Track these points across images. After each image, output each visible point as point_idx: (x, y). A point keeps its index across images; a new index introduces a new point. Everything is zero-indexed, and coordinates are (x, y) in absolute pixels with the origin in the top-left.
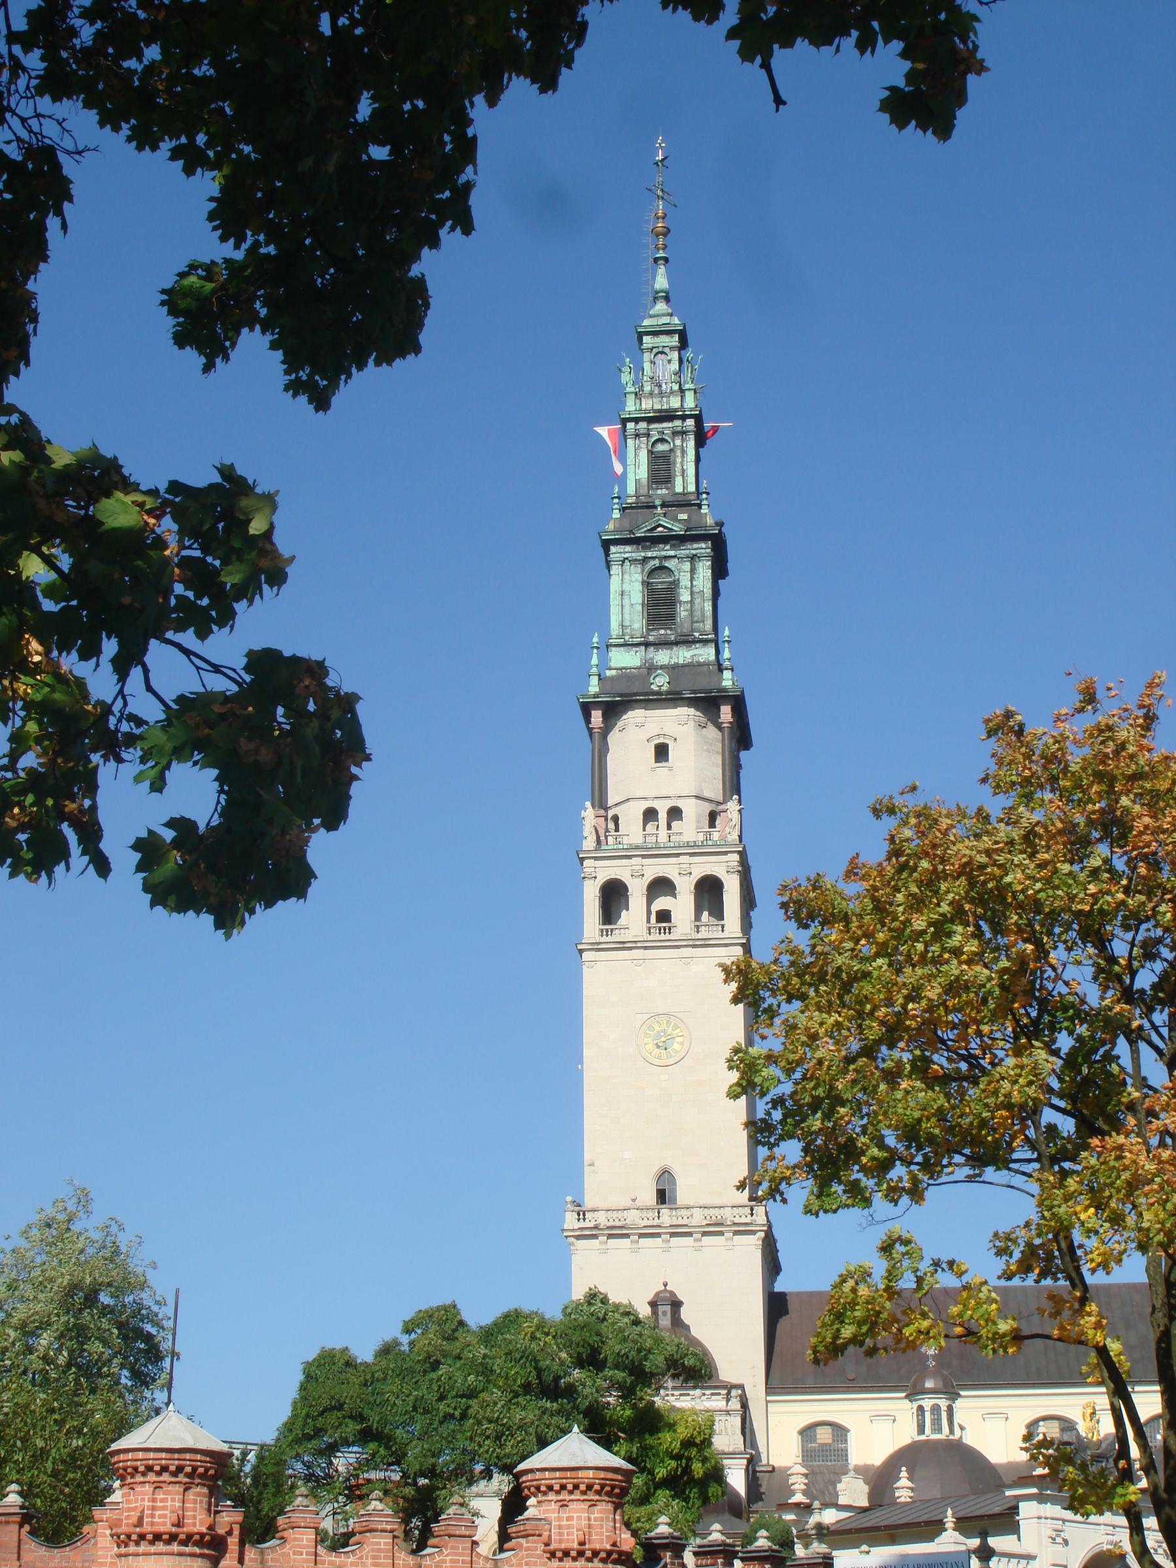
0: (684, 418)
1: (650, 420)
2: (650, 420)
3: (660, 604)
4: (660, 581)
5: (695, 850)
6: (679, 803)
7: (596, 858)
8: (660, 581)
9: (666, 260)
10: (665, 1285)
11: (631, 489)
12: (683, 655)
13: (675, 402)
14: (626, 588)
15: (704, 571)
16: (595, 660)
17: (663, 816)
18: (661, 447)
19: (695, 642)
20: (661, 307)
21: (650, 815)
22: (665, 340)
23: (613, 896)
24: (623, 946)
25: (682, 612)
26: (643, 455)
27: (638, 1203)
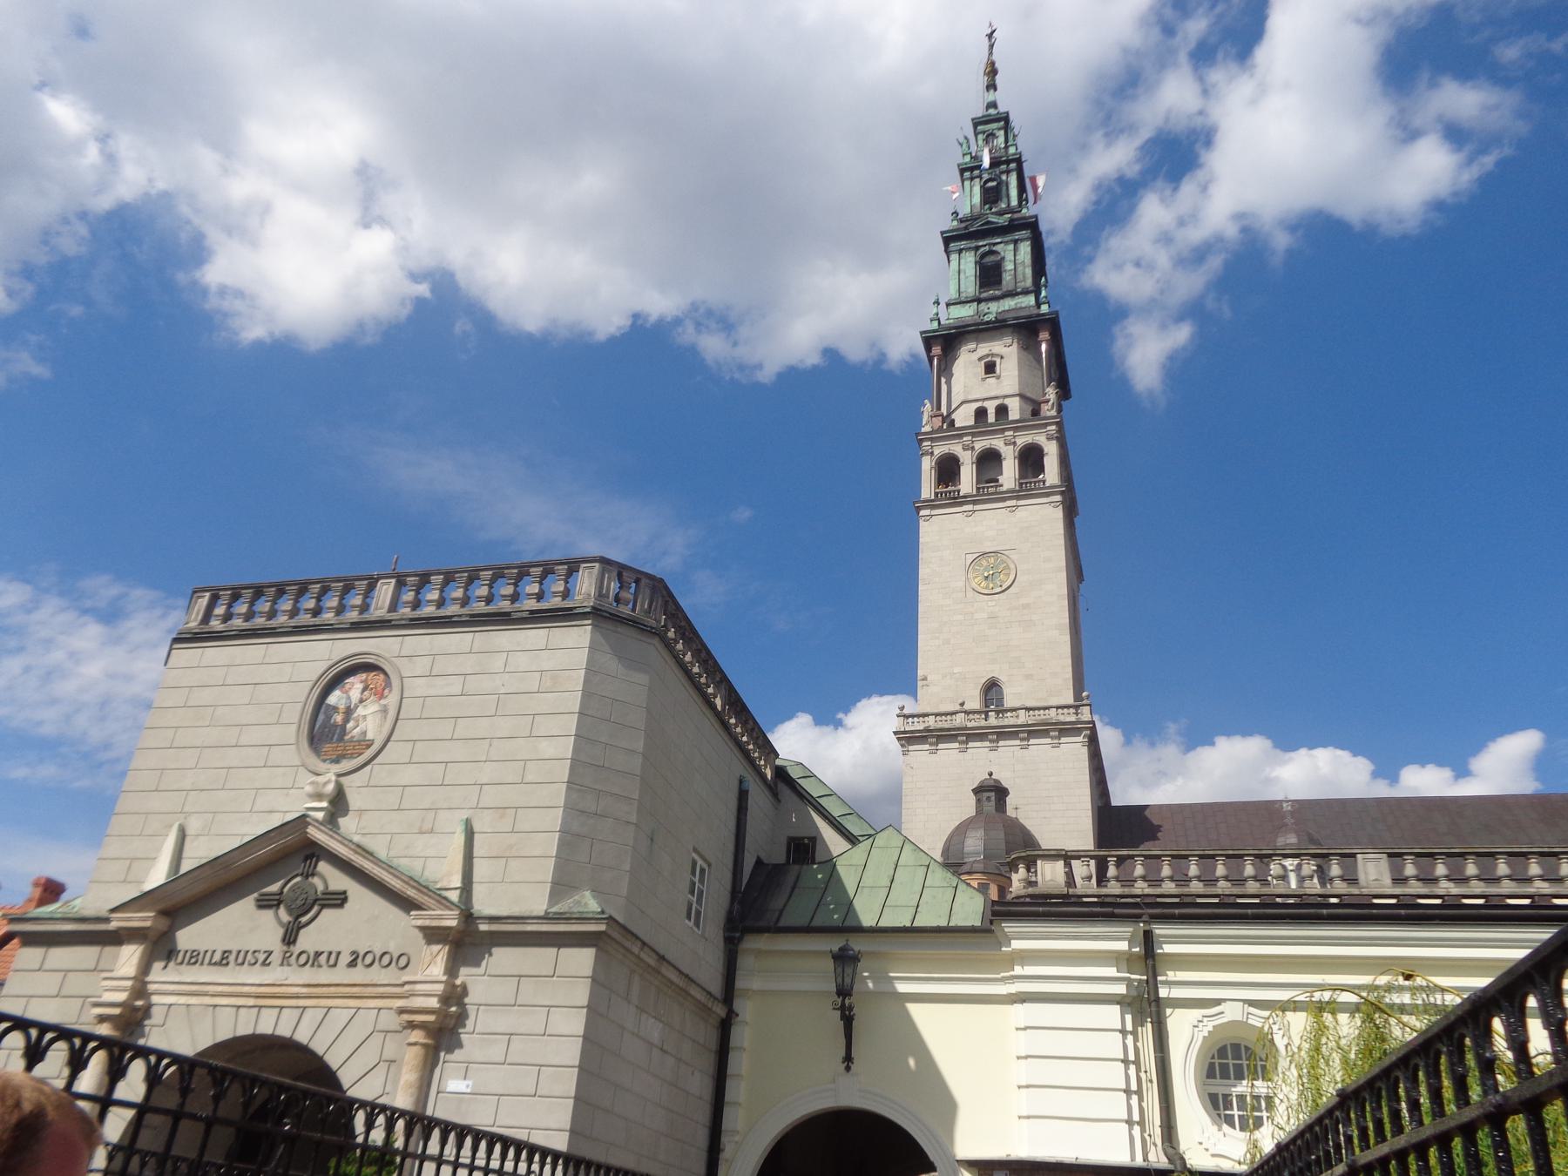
0: (1008, 162)
3: (990, 275)
4: (990, 259)
5: (1019, 427)
6: (1007, 401)
8: (990, 259)
10: (991, 774)
12: (1008, 304)
15: (1025, 249)
19: (1017, 294)
21: (981, 414)
22: (995, 125)
23: (948, 470)
24: (957, 500)
25: (1007, 278)
26: (977, 190)
27: (966, 707)
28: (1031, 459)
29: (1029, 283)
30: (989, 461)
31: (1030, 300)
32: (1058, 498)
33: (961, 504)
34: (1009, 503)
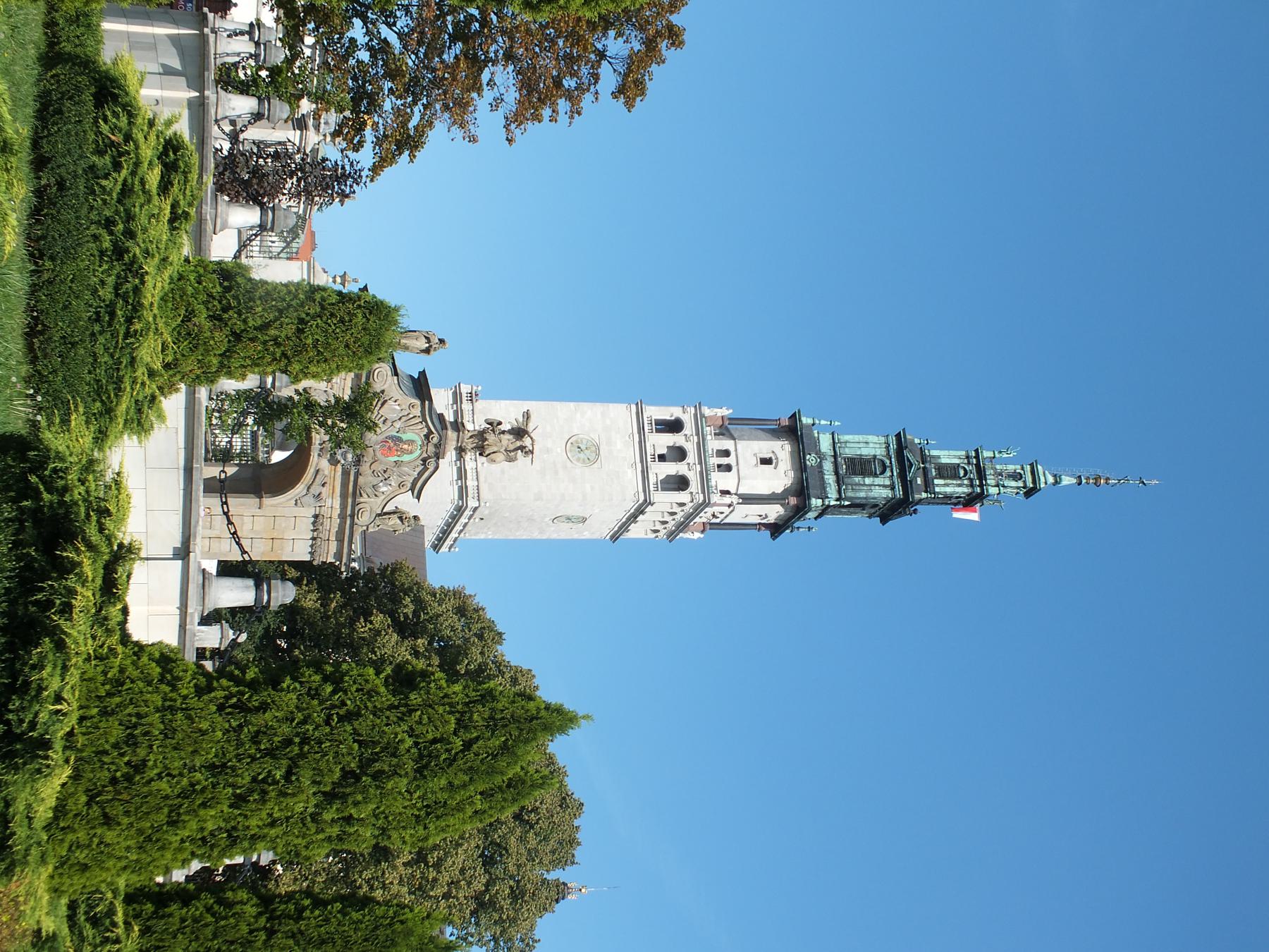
0: (981, 486)
1: (978, 465)
2: (978, 465)
3: (861, 466)
5: (704, 478)
6: (734, 469)
7: (696, 415)
9: (1080, 484)
11: (934, 453)
12: (830, 478)
13: (991, 481)
14: (872, 445)
15: (887, 493)
16: (823, 422)
17: (724, 461)
18: (962, 473)
20: (1051, 480)
21: (726, 453)
23: (674, 426)
24: (641, 429)
25: (857, 479)
26: (957, 461)
28: (680, 483)
29: (850, 494)
30: (679, 454)
31: (832, 492)
32: (642, 499)
33: (639, 433)
34: (639, 465)
